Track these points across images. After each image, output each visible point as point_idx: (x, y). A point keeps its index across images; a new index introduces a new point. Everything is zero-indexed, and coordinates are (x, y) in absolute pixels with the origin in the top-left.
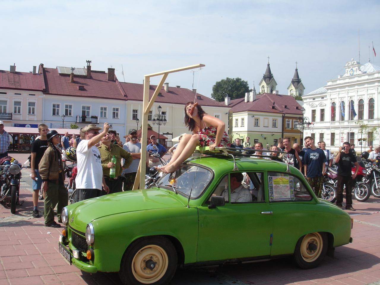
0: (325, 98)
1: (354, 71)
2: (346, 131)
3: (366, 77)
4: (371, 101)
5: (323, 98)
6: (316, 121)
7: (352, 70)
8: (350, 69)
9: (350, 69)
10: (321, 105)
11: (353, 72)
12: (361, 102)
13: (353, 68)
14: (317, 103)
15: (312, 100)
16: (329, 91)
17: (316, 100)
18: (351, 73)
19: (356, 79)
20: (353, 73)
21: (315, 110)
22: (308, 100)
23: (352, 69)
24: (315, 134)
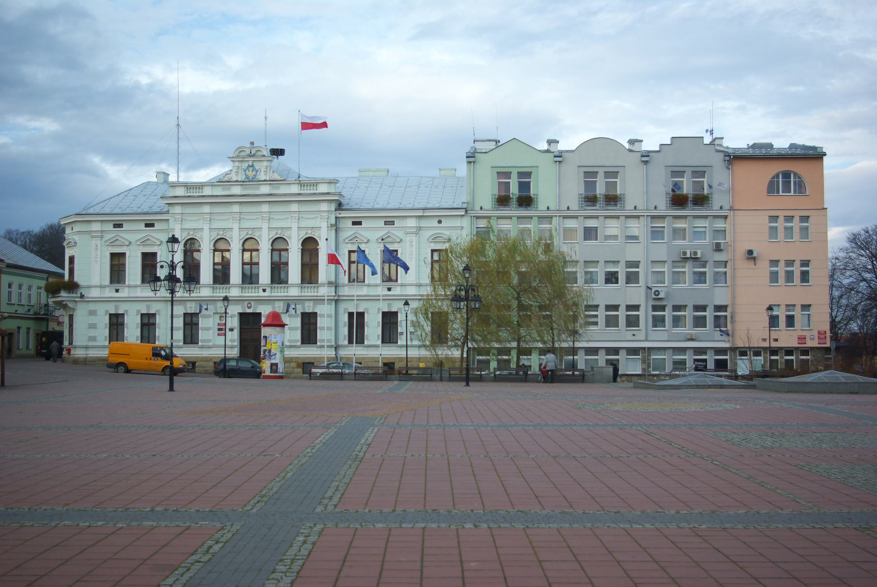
0: (157, 226)
1: (257, 171)
2: (235, 310)
3: (295, 189)
4: (309, 246)
5: (149, 225)
6: (127, 283)
7: (251, 169)
8: (245, 165)
9: (245, 165)
10: (144, 243)
11: (254, 173)
12: (279, 246)
13: (255, 164)
14: (133, 237)
15: (110, 227)
16: (178, 210)
17: (126, 227)
18: (250, 174)
19: (265, 189)
20: (255, 176)
21: (124, 254)
22: (96, 227)
23: (252, 166)
24: (123, 314)
